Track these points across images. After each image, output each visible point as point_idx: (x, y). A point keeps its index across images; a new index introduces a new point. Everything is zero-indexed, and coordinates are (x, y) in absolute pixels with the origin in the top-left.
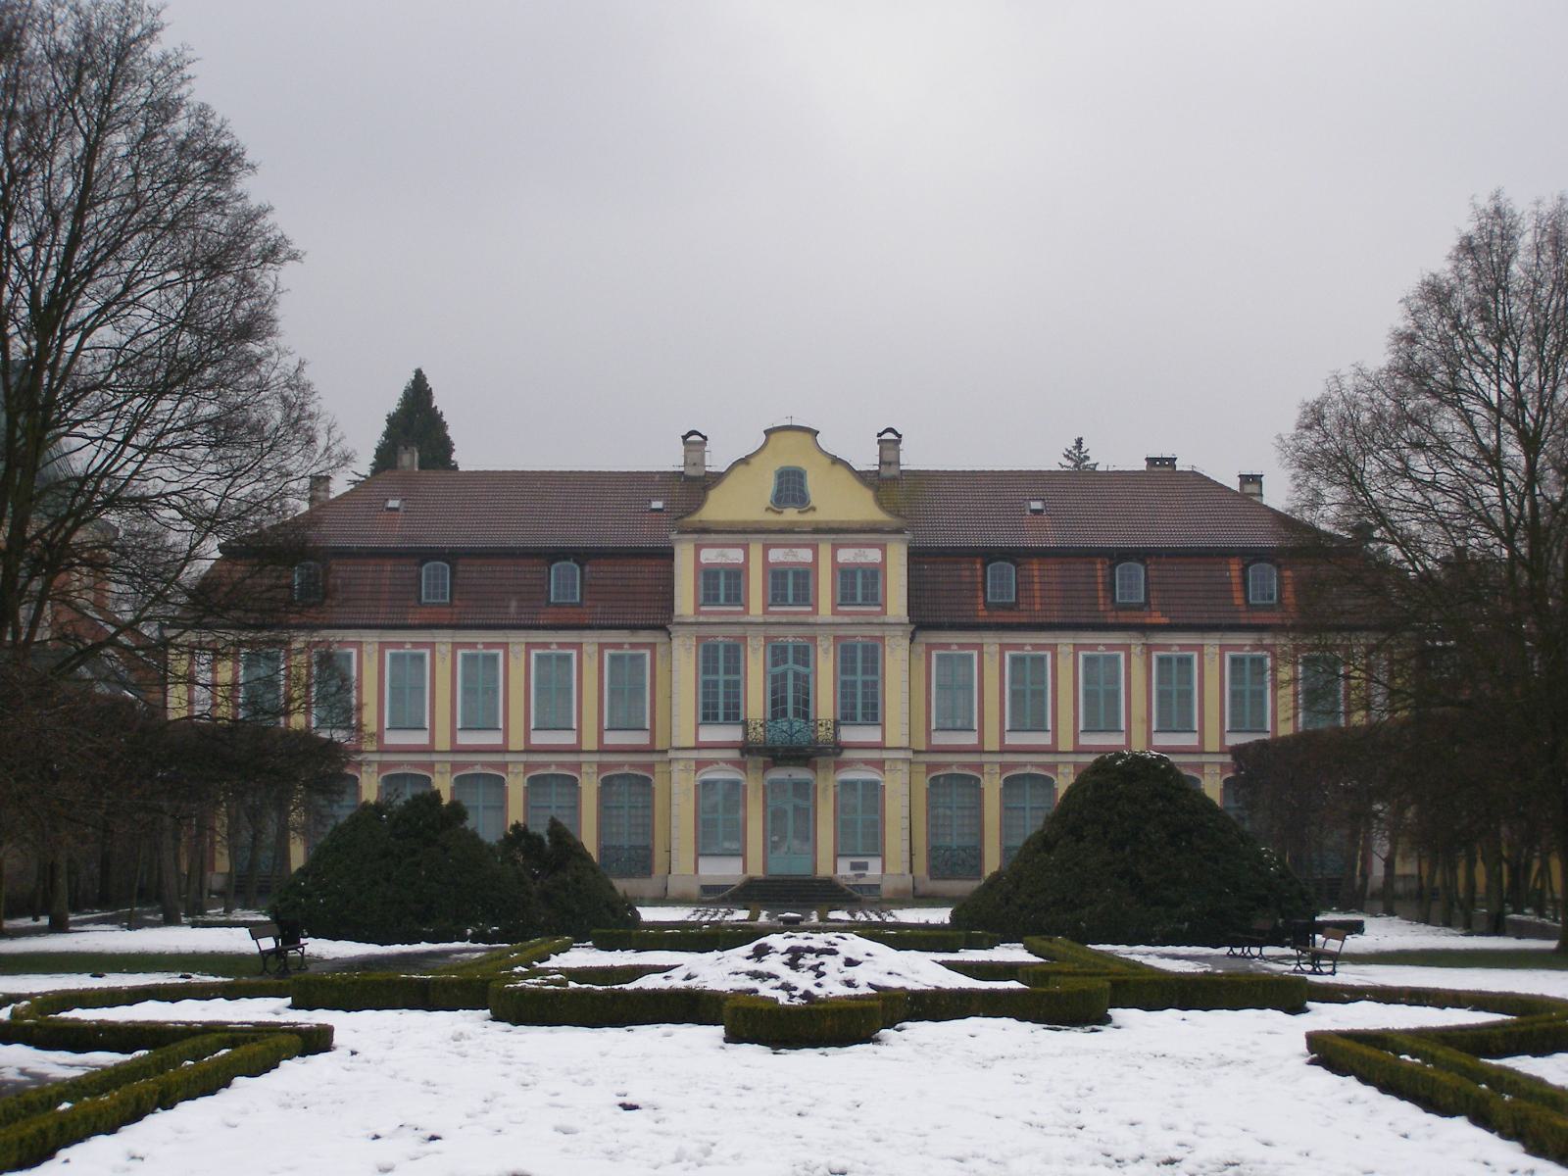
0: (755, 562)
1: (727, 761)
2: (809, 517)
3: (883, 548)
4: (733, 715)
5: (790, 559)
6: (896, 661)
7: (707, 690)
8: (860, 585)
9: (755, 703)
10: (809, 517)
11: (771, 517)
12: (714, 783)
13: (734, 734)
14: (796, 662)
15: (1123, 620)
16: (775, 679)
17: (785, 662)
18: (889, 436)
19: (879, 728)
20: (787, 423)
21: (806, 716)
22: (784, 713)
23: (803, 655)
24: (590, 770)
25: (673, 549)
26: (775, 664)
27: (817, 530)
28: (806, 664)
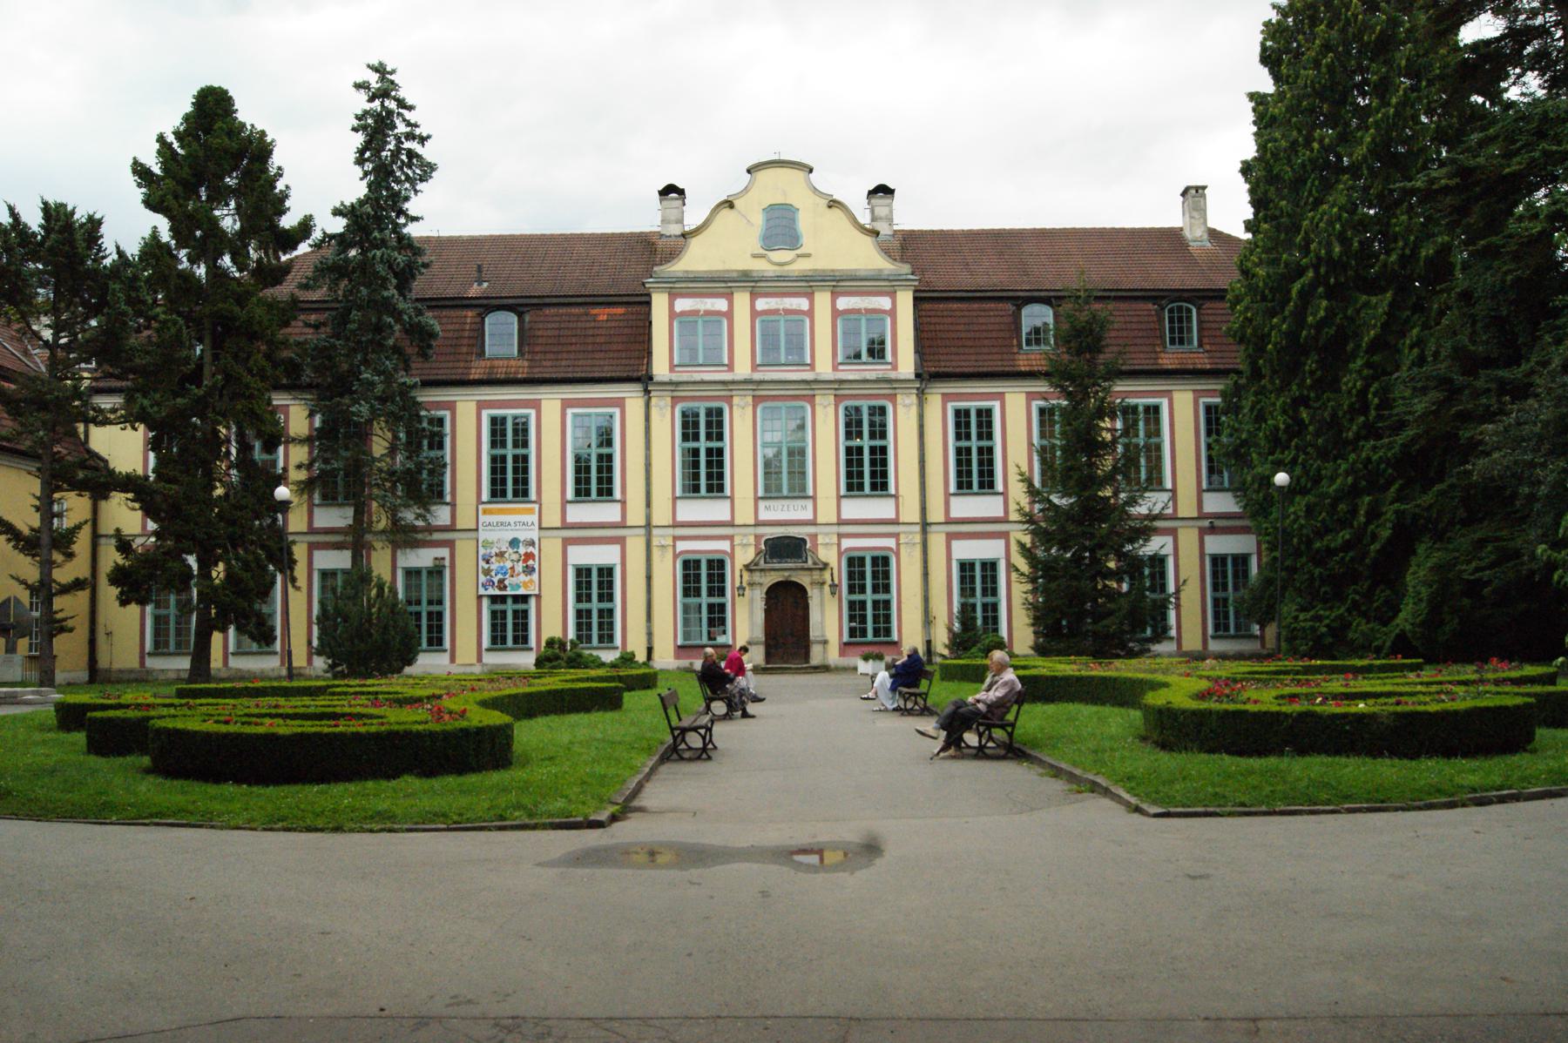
2: (803, 266)
3: (892, 295)
6: (903, 419)
19: (892, 502)
20: (776, 157)
25: (649, 295)
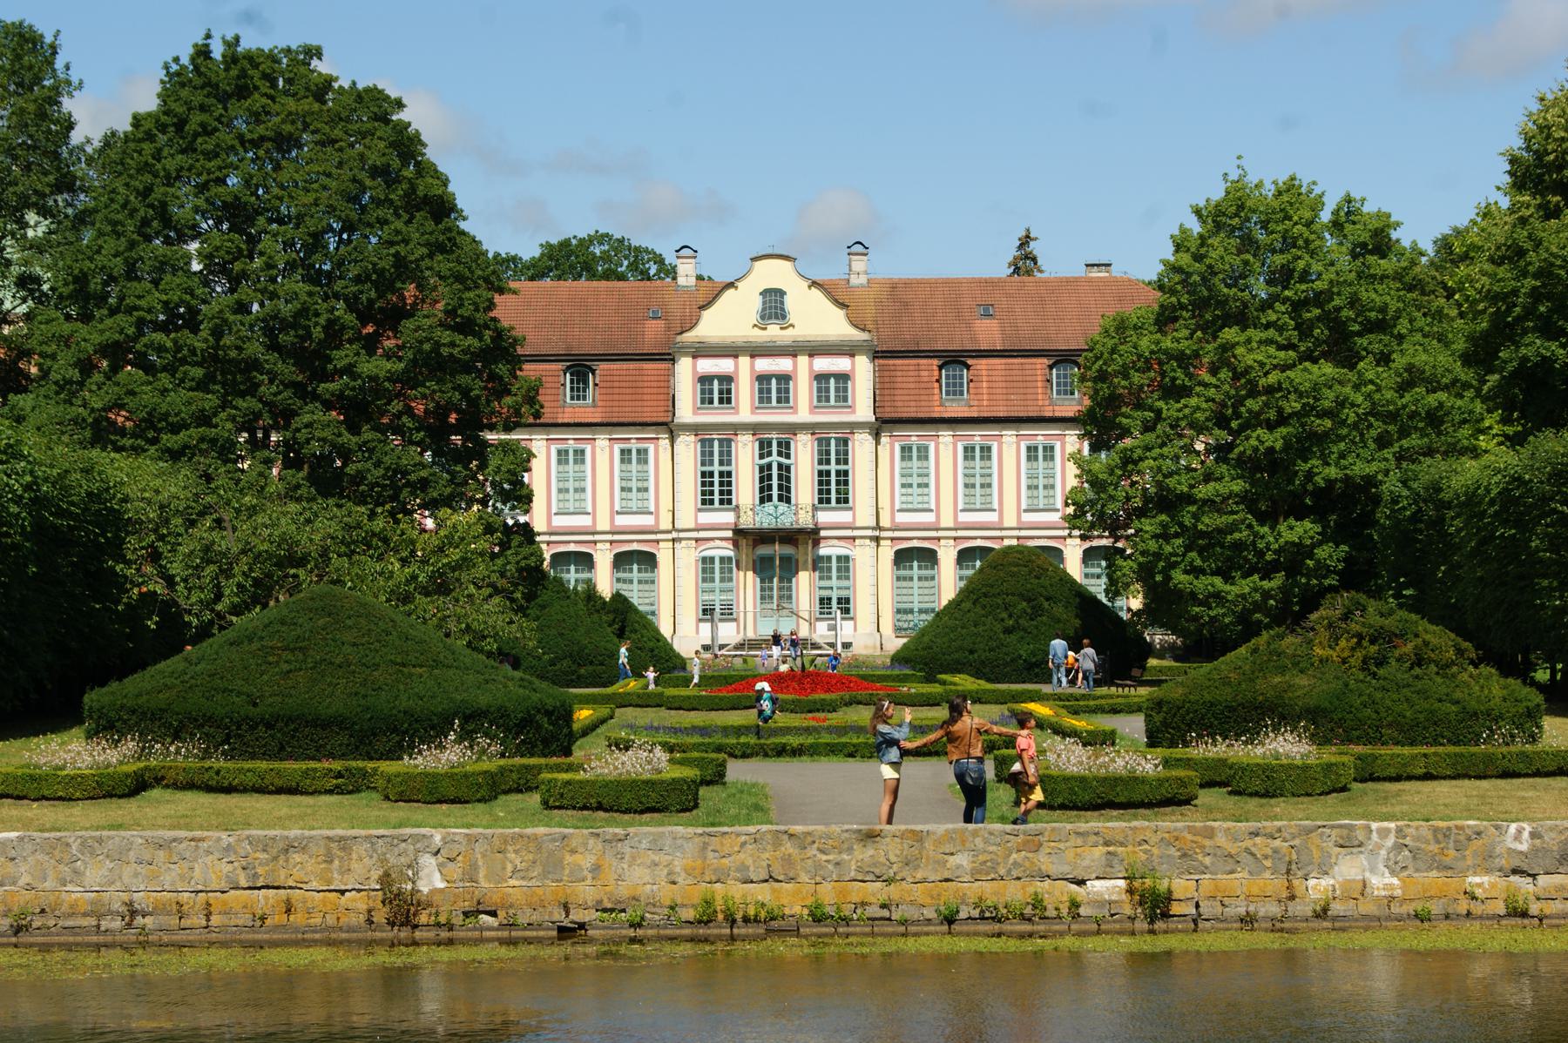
0: (744, 370)
1: (721, 539)
8: (832, 387)
9: (746, 488)
10: (790, 331)
11: (757, 332)
12: (712, 559)
13: (727, 517)
14: (780, 454)
15: (1057, 414)
16: (761, 469)
17: (770, 454)
18: (859, 248)
21: (788, 501)
22: (770, 498)
26: (761, 457)
28: (788, 456)
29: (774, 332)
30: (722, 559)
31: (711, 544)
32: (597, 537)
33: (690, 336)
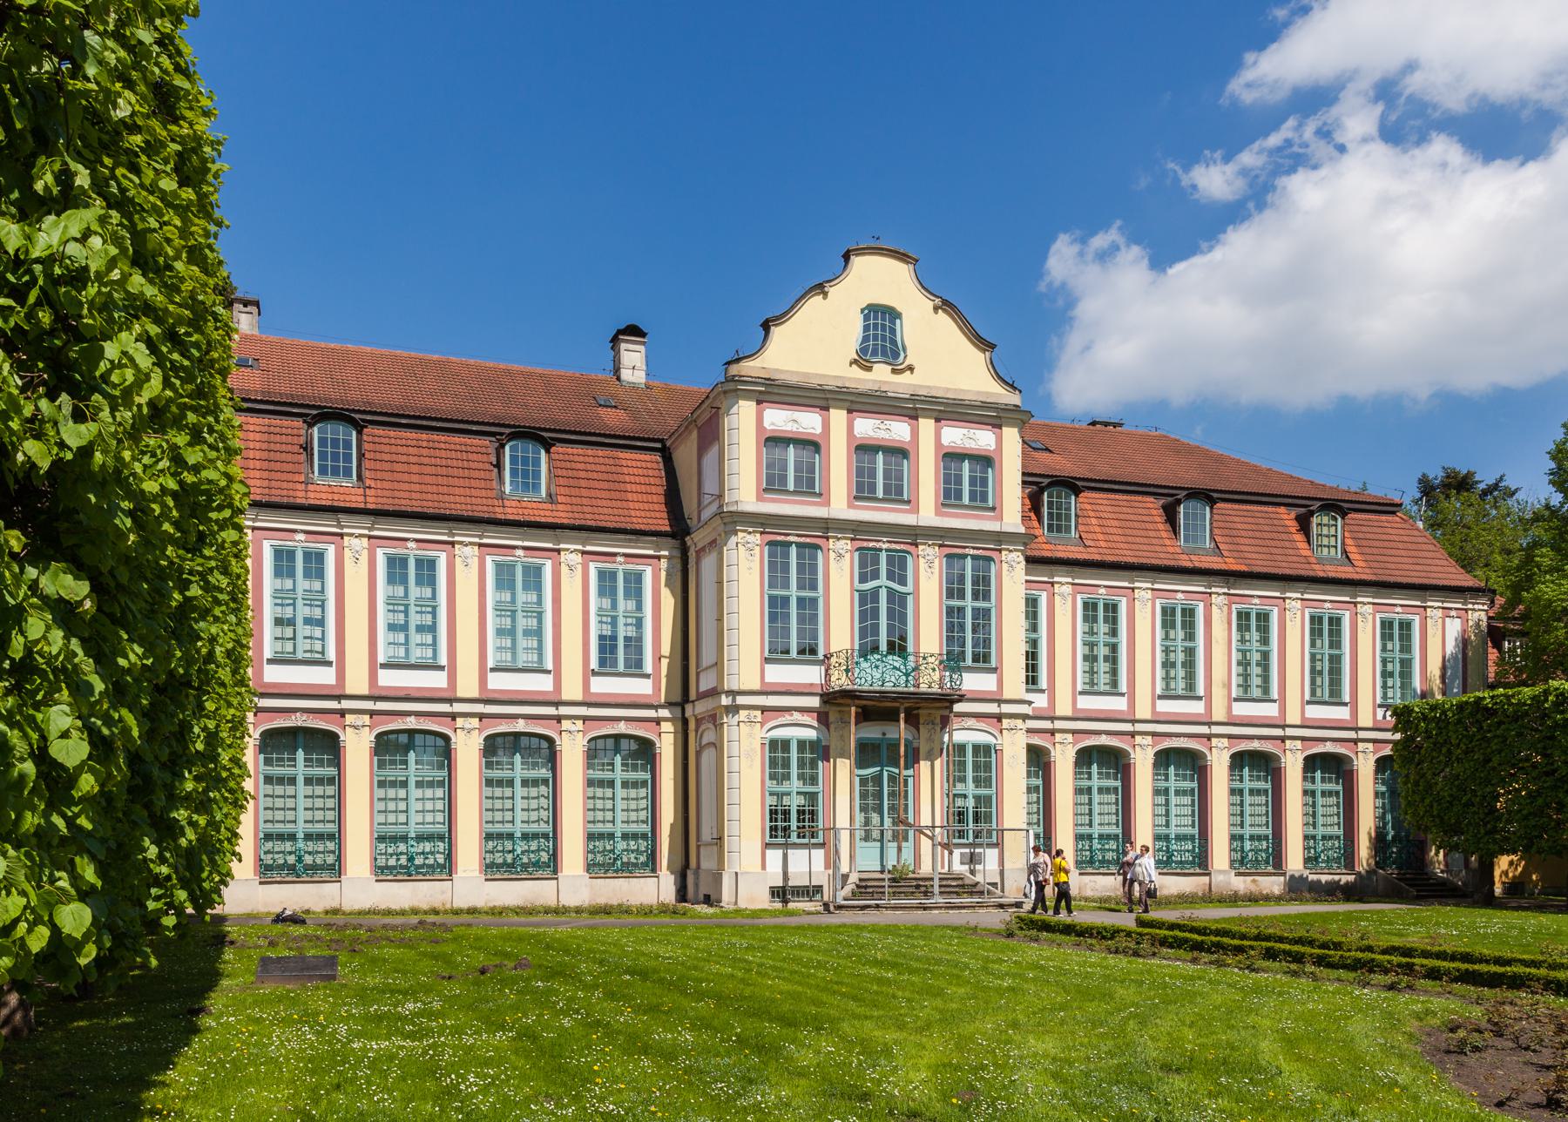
2: (902, 384)
4: (808, 651)
5: (882, 434)
7: (776, 608)
12: (786, 744)
14: (890, 577)
17: (876, 576)
23: (898, 570)
24: (573, 728)
26: (863, 579)
27: (914, 398)
28: (903, 582)
29: (880, 375)
30: (802, 744)
31: (787, 718)
32: (563, 710)
33: (750, 368)
